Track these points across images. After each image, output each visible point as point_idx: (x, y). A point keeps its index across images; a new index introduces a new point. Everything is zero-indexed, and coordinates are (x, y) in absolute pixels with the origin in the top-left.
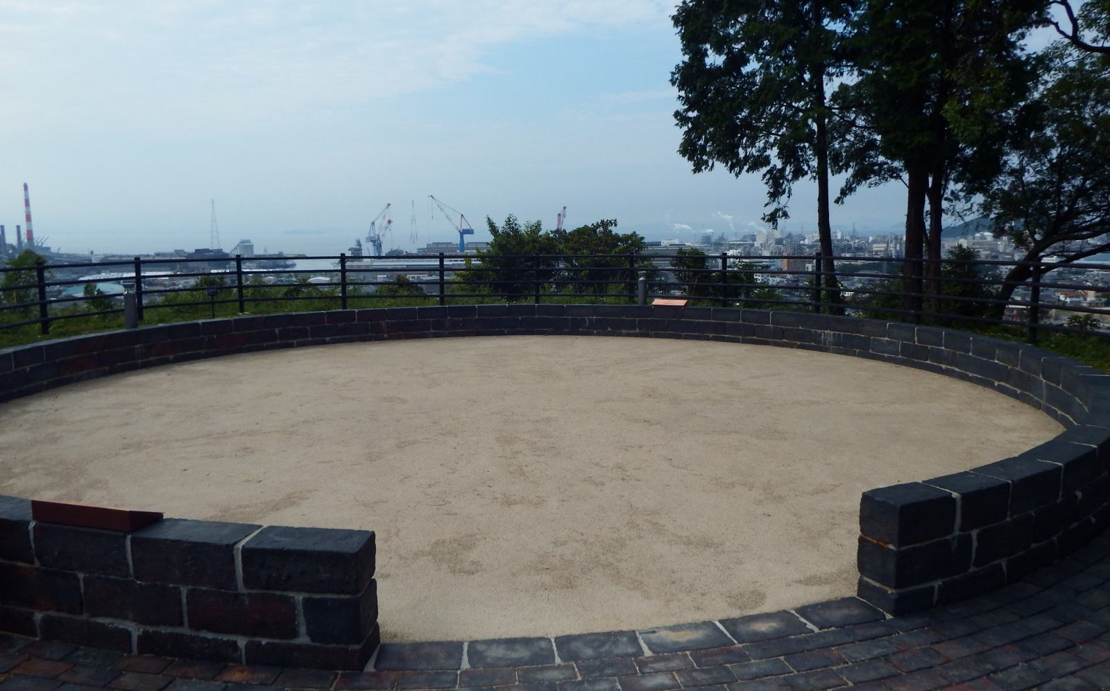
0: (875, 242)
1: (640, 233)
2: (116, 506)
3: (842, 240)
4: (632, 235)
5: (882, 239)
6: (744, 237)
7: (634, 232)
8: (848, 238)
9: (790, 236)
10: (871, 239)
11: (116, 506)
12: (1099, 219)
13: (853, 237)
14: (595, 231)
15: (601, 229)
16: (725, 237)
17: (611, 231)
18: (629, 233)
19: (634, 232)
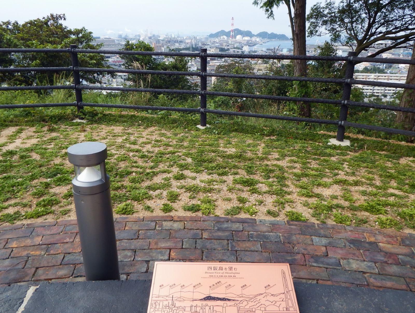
0: (186, 39)
1: (89, 29)
2: (152, 305)
3: (174, 38)
4: (82, 30)
5: (190, 38)
6: (136, 36)
7: (84, 28)
8: (176, 37)
9: (154, 36)
10: (185, 38)
11: (152, 305)
12: (21, 179)
13: (178, 37)
14: (46, 23)
15: (52, 21)
16: (128, 35)
17: (61, 25)
18: (80, 28)
19: (84, 28)
